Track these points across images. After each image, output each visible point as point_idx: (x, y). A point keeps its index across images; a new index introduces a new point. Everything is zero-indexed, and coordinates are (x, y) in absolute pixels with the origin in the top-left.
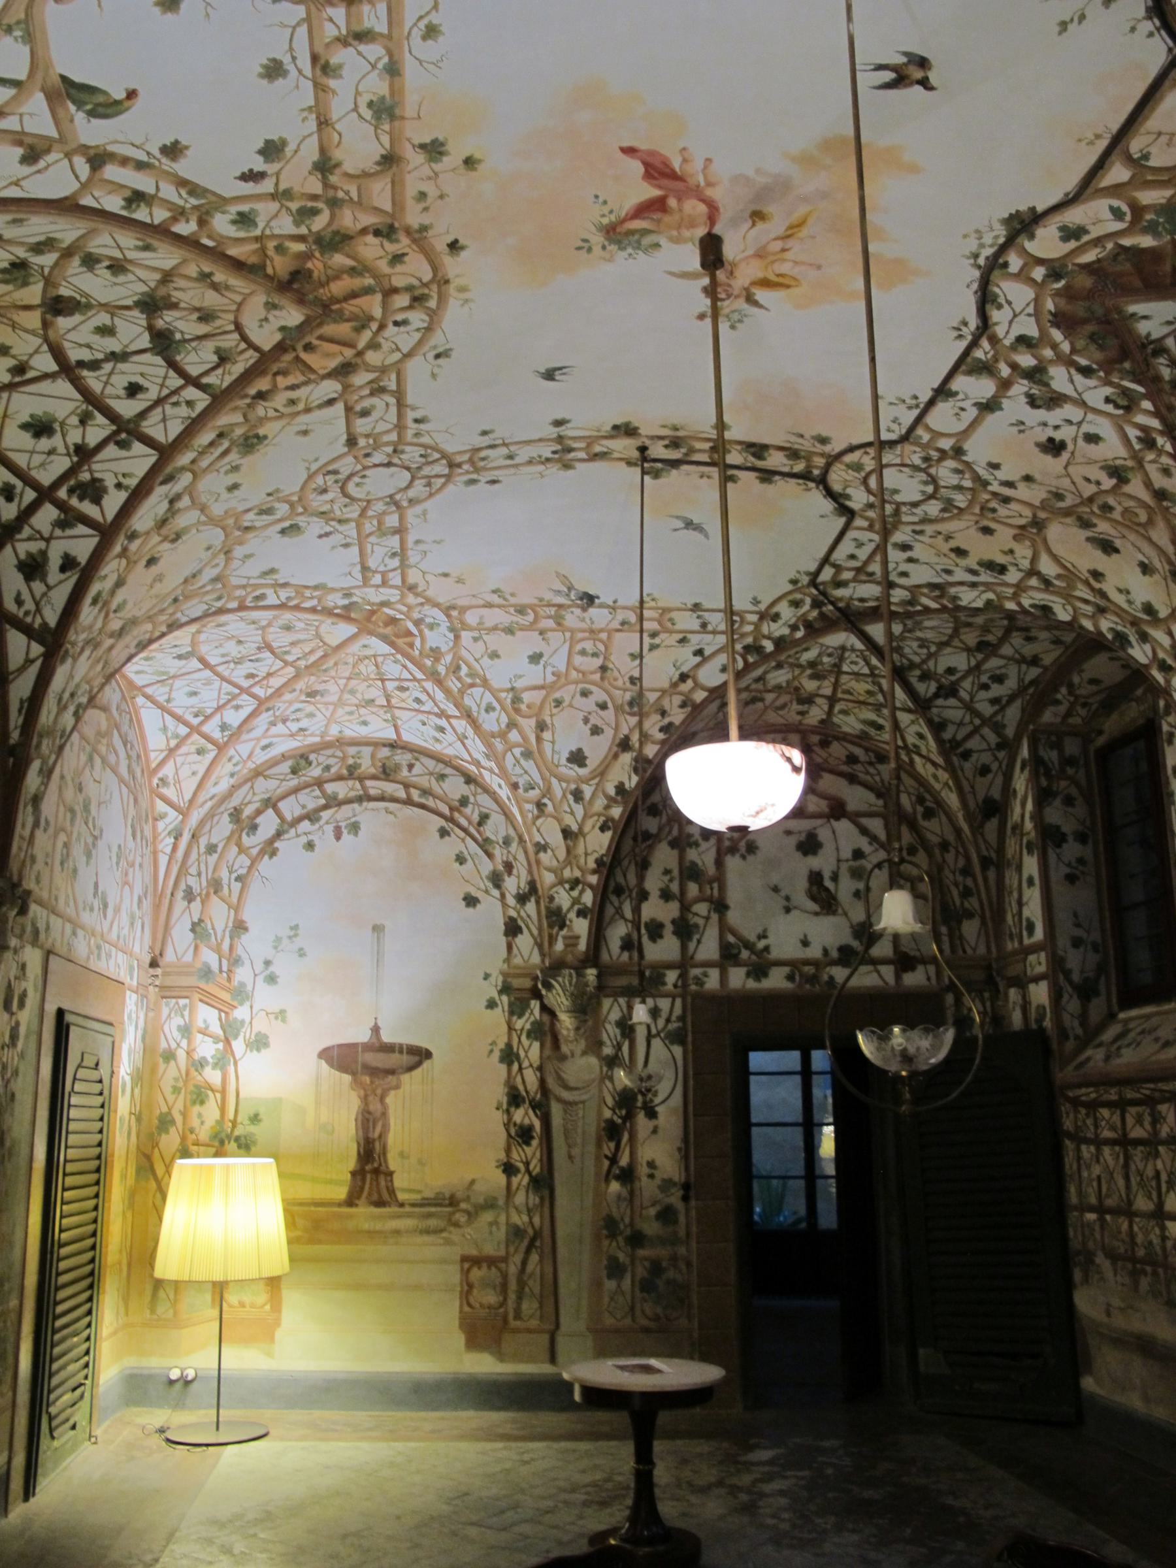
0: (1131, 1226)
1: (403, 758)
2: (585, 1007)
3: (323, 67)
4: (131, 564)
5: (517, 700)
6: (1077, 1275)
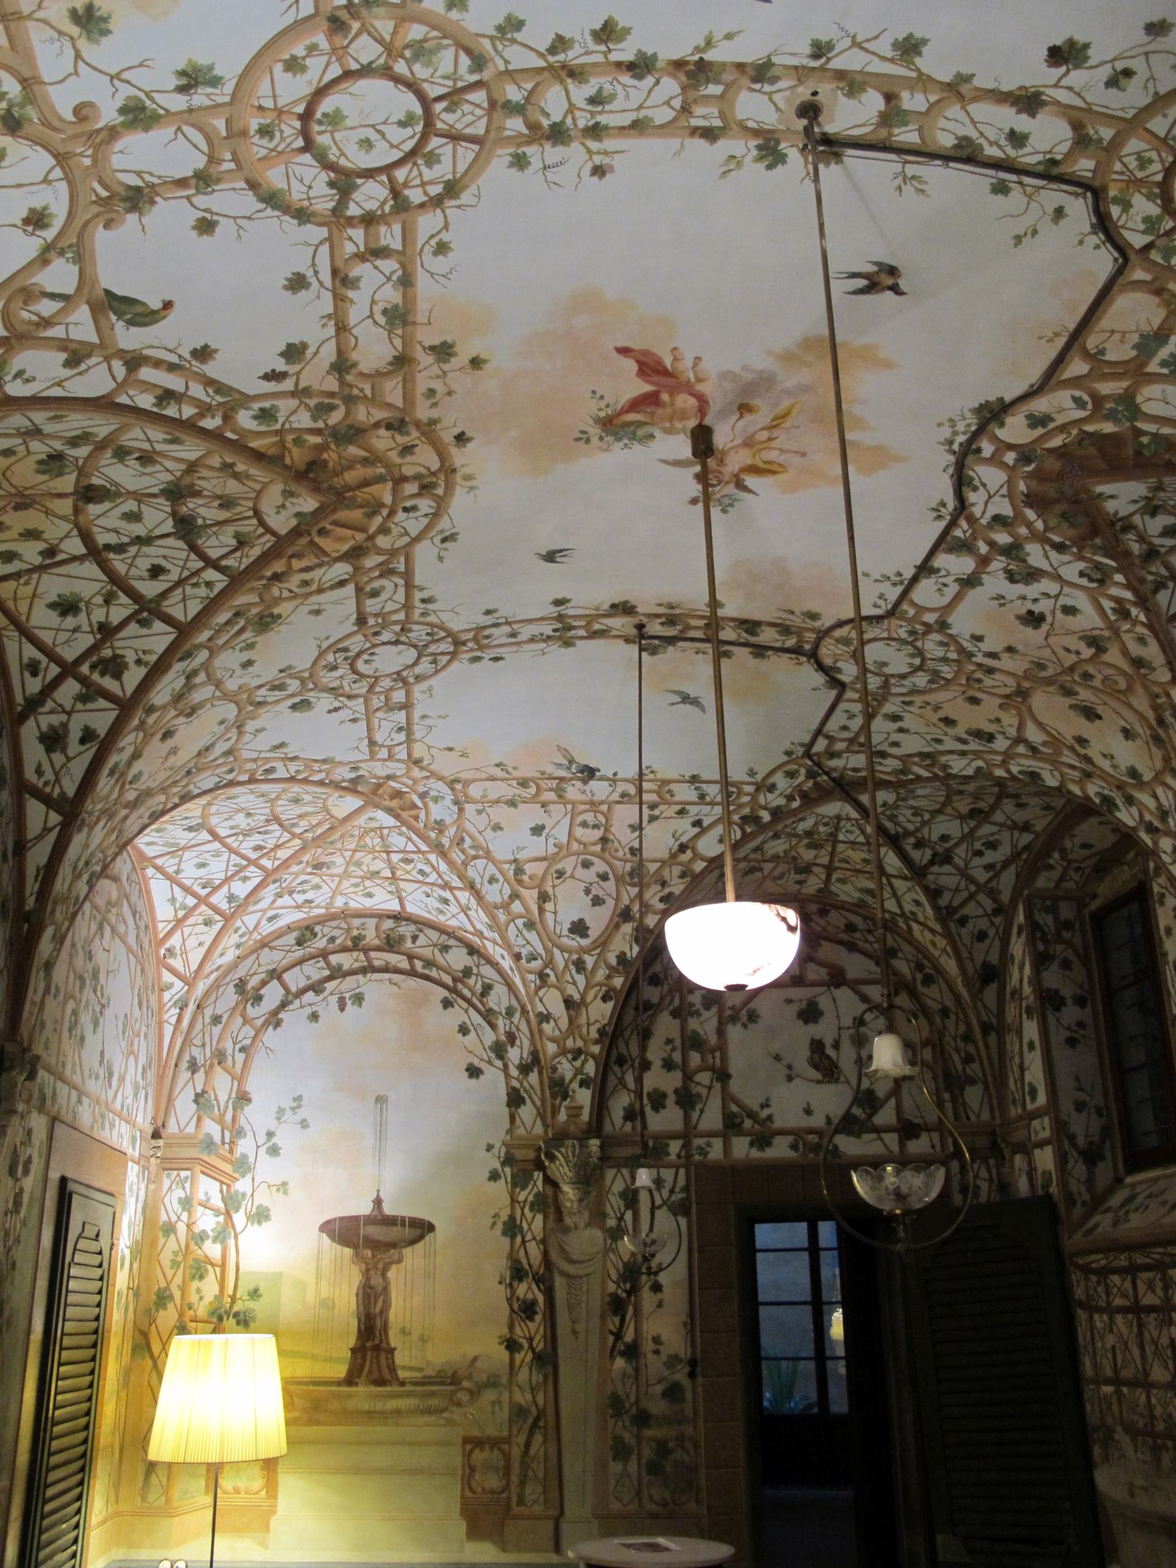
1: (407, 930)
2: (588, 1178)
3: (342, 280)
4: (148, 737)
5: (519, 871)
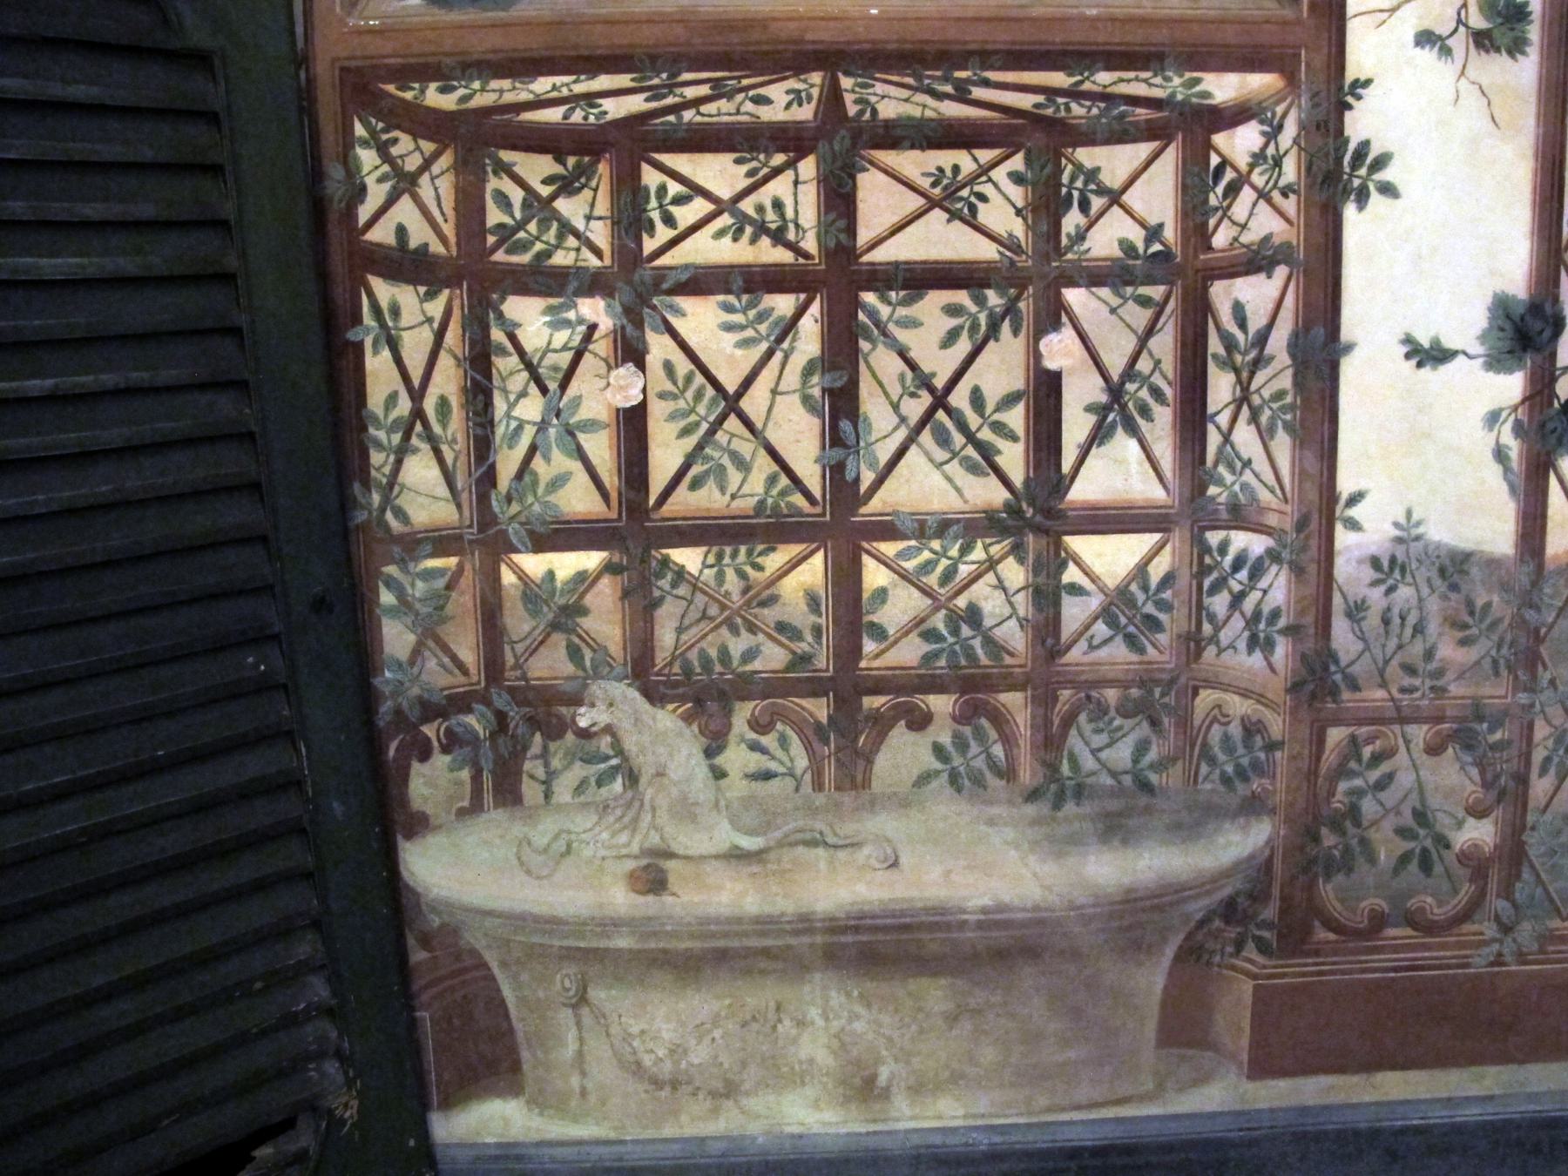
0: (845, 577)
6: (432, 782)
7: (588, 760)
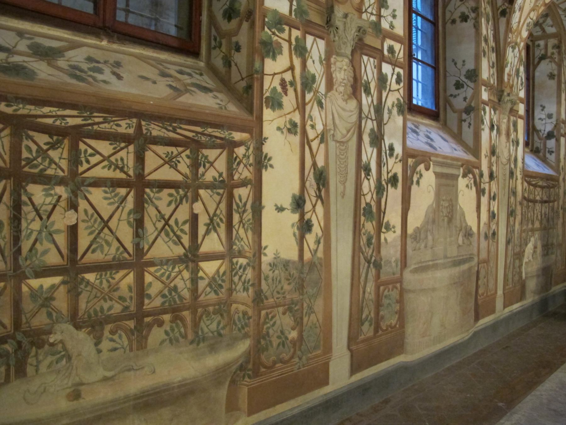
0: (140, 279)
7: (53, 355)
